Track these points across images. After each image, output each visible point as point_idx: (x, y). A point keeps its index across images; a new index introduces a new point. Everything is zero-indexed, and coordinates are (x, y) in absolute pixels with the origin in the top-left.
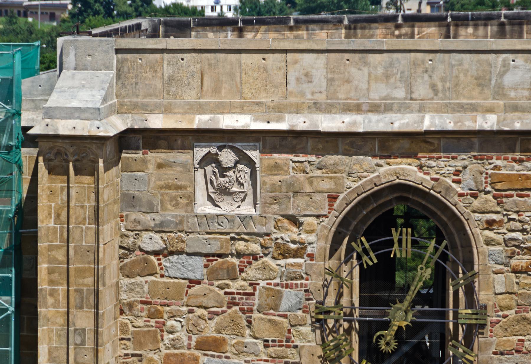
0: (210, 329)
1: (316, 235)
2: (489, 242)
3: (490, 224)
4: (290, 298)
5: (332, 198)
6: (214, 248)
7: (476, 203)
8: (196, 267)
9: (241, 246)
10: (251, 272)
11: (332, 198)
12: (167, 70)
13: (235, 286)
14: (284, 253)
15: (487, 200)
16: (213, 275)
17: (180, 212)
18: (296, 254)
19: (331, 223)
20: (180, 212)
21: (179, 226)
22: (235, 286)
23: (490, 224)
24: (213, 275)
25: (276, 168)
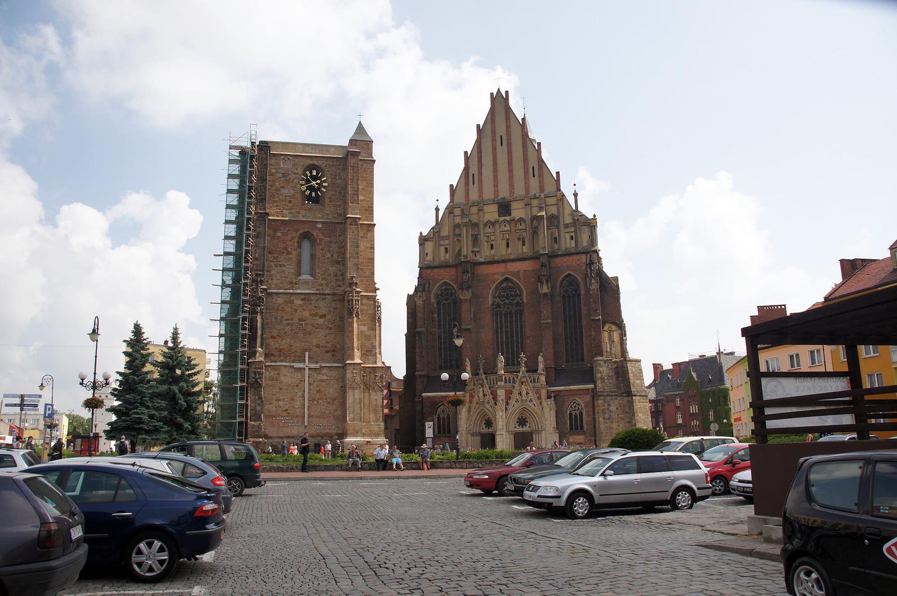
1: (300, 171)
4: (296, 181)
8: (281, 175)
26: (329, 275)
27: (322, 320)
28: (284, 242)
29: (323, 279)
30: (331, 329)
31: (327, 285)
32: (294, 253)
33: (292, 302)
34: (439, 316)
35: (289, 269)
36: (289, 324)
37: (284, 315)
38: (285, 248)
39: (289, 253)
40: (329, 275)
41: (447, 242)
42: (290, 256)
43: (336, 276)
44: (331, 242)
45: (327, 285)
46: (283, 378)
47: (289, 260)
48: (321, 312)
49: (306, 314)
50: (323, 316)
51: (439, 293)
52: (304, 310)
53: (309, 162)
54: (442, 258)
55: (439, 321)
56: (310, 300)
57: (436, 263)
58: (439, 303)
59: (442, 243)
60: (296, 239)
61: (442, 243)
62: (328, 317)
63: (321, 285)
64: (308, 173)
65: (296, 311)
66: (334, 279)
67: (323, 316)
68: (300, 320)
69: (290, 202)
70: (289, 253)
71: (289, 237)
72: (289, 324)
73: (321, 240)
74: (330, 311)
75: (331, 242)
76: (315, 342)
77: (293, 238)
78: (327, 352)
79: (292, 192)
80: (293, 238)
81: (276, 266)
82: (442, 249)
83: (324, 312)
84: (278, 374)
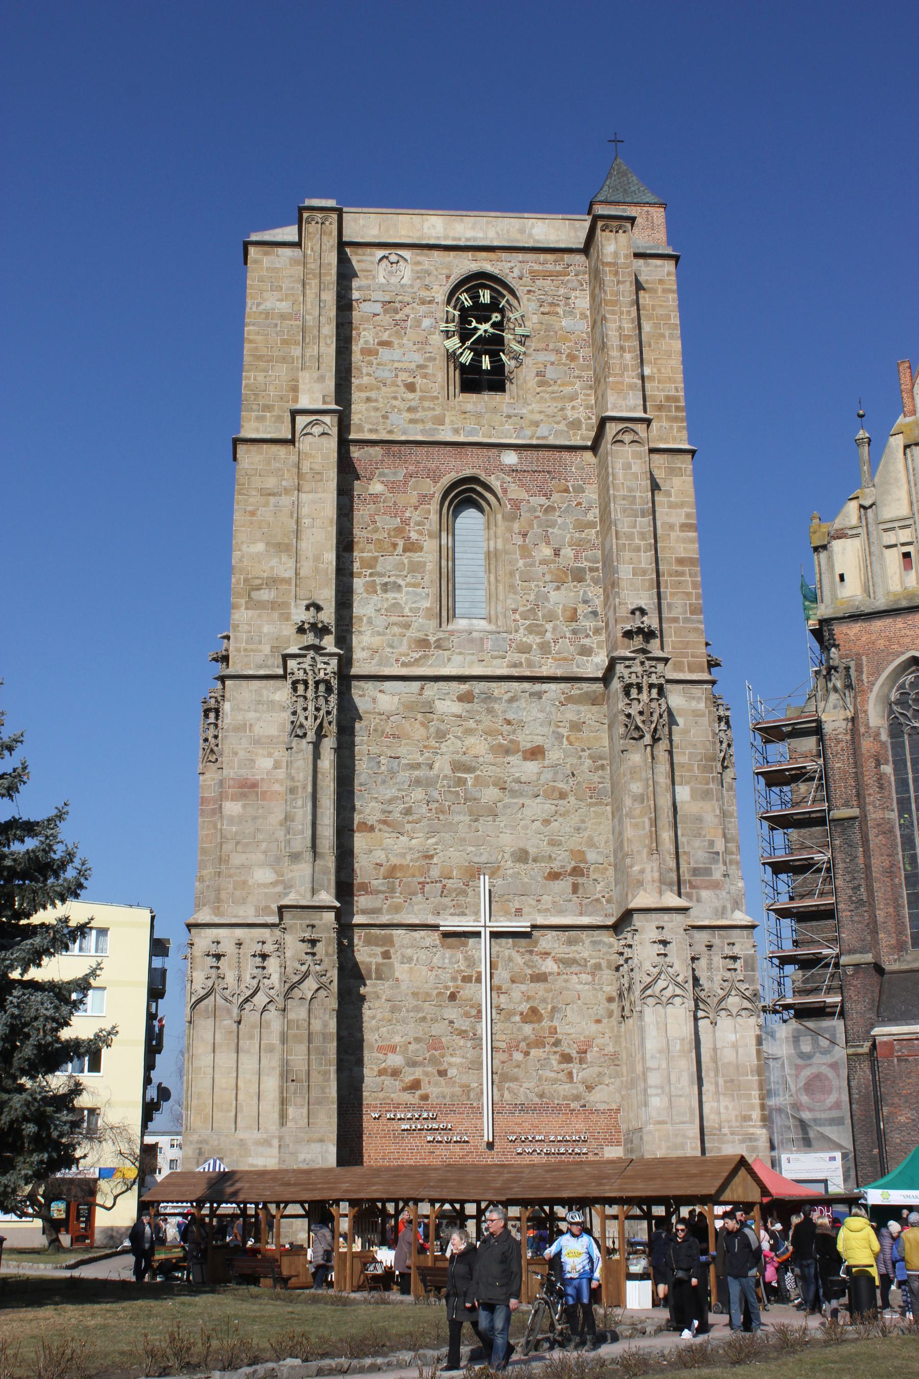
0: (385, 337)
1: (440, 294)
2: (529, 300)
3: (529, 292)
4: (426, 323)
5: (448, 277)
6: (387, 299)
7: (521, 282)
8: (378, 308)
9: (400, 298)
10: (407, 310)
11: (448, 277)
12: (361, 222)
13: (397, 317)
14: (423, 302)
15: (527, 280)
16: (386, 312)
17: (369, 282)
18: (430, 302)
19: (447, 288)
20: (369, 282)
21: (368, 288)
22: (397, 317)
23: (529, 292)
24: (386, 312)
25: (418, 263)
26: (550, 617)
27: (532, 767)
28: (395, 511)
29: (530, 630)
30: (563, 795)
31: (545, 648)
32: (430, 545)
33: (428, 709)
34: (899, 765)
35: (418, 599)
36: (418, 782)
37: (402, 751)
38: (399, 531)
39: (412, 547)
40: (550, 617)
41: (904, 535)
42: (416, 557)
43: (573, 618)
44: (549, 510)
45: (545, 648)
46: (401, 970)
47: (416, 568)
48: (526, 740)
49: (478, 746)
50: (536, 753)
51: (894, 696)
52: (469, 732)
53: (467, 264)
54: (895, 586)
55: (902, 784)
56: (489, 698)
57: (881, 603)
58: (896, 730)
59: (890, 538)
60: (434, 506)
61: (890, 538)
62: (554, 755)
63: (525, 649)
64: (464, 297)
65: (441, 736)
66: (566, 630)
67: (536, 753)
68: (458, 766)
69: (411, 387)
70: (412, 547)
71: (413, 497)
72: (418, 782)
73: (516, 504)
74: (559, 737)
75: (549, 510)
76: (509, 841)
77: (424, 499)
78: (554, 876)
79: (418, 358)
80: (424, 499)
81: (371, 588)
82: (893, 558)
83: (539, 741)
84: (386, 955)
